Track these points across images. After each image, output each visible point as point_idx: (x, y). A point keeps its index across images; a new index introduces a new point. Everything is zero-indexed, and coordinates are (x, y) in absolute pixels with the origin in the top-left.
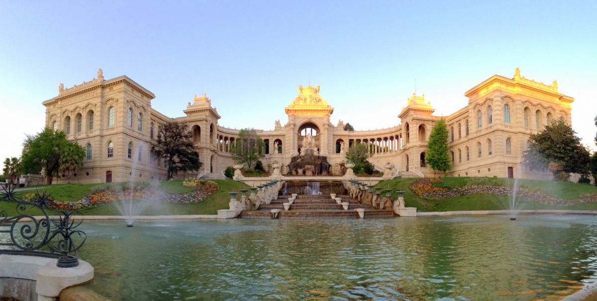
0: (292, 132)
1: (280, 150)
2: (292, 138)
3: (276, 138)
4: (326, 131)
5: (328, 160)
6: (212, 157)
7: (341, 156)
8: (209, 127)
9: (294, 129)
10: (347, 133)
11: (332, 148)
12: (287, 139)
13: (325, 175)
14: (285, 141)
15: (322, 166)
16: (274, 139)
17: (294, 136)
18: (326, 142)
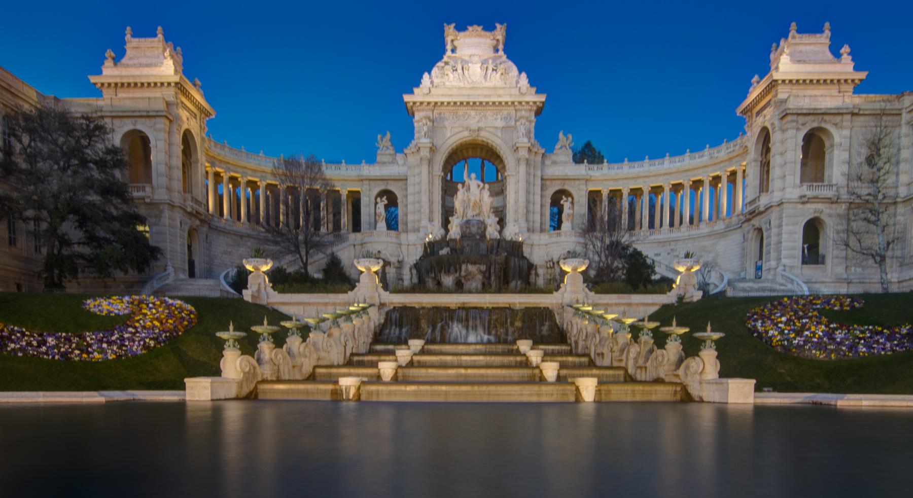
0: (425, 169)
1: (392, 224)
2: (425, 187)
3: (381, 187)
4: (523, 168)
5: (526, 251)
6: (191, 233)
7: (563, 238)
8: (178, 139)
9: (430, 162)
10: (582, 170)
11: (538, 217)
12: (410, 189)
13: (521, 291)
14: (406, 196)
15: (509, 266)
16: (376, 191)
17: (431, 183)
18: (522, 199)
